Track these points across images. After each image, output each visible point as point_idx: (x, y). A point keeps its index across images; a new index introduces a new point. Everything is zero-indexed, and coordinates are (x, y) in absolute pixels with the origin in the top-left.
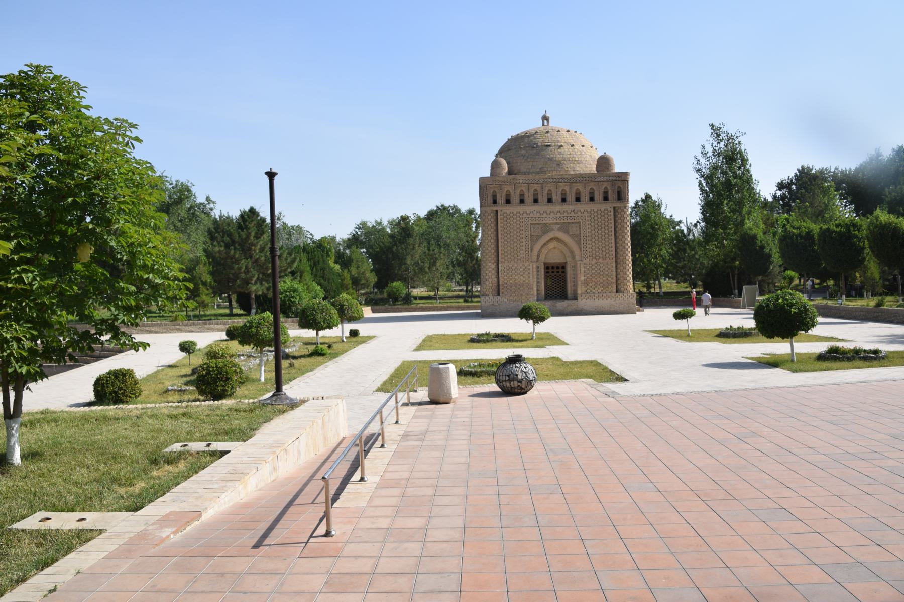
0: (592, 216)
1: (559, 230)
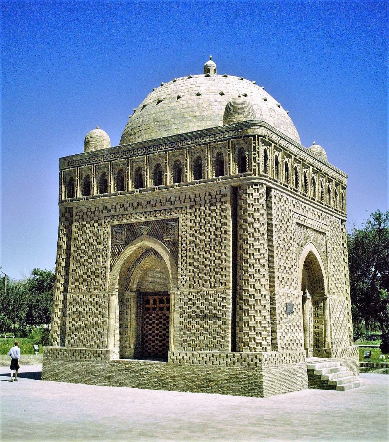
1: (148, 234)
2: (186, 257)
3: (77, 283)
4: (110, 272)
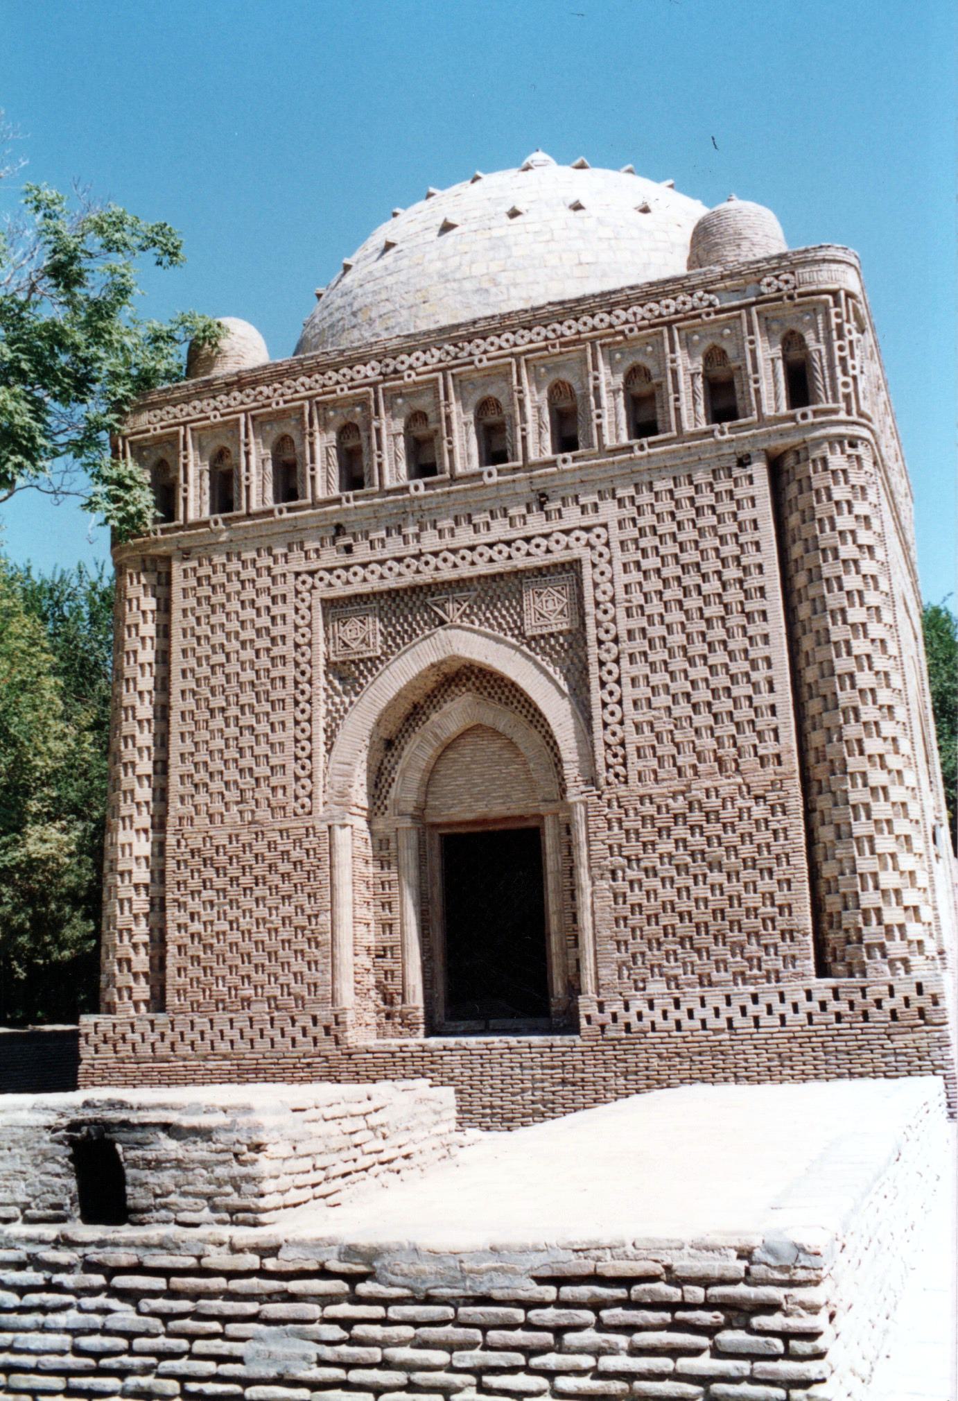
0: (647, 520)
2: (618, 682)
3: (202, 798)
4: (329, 751)
